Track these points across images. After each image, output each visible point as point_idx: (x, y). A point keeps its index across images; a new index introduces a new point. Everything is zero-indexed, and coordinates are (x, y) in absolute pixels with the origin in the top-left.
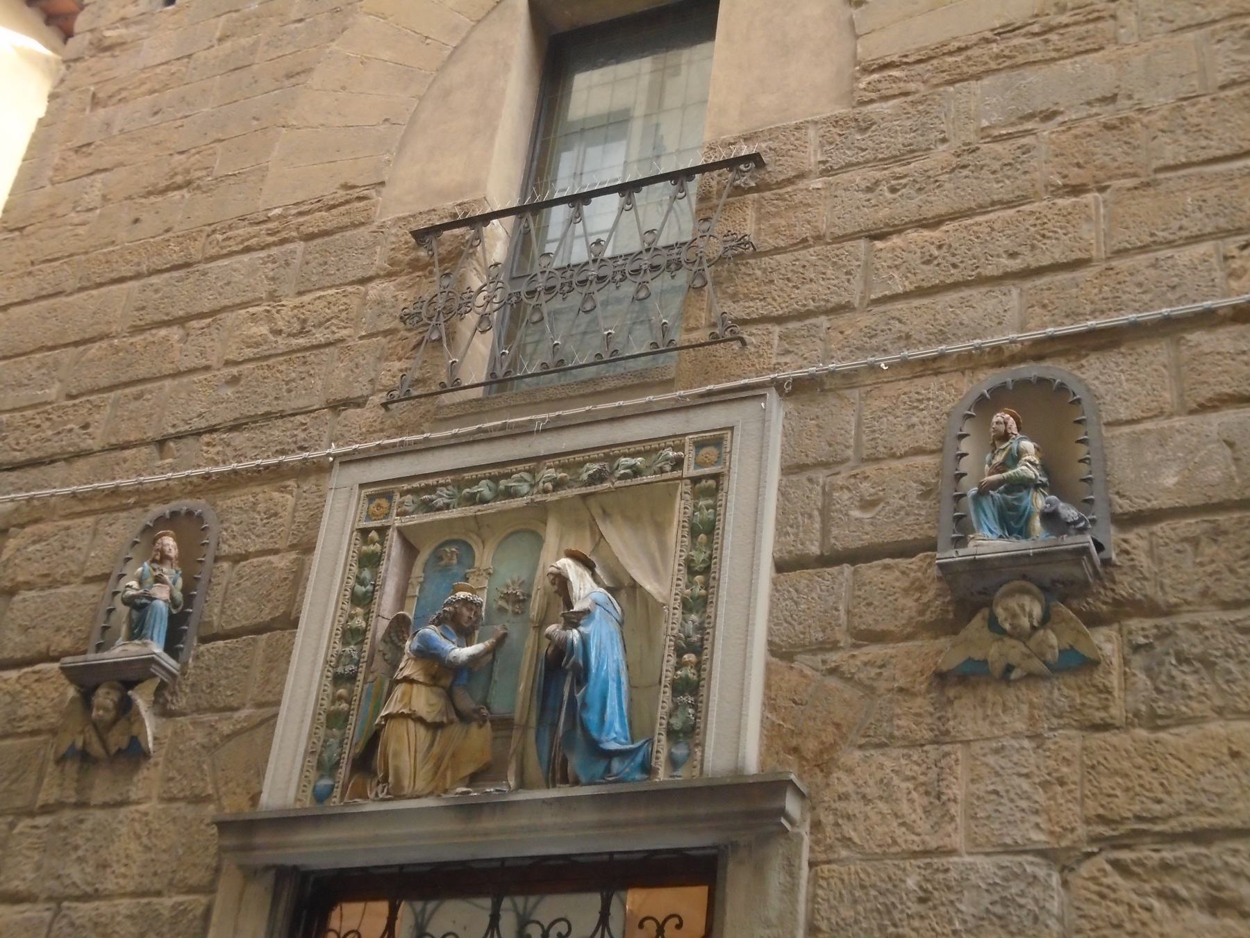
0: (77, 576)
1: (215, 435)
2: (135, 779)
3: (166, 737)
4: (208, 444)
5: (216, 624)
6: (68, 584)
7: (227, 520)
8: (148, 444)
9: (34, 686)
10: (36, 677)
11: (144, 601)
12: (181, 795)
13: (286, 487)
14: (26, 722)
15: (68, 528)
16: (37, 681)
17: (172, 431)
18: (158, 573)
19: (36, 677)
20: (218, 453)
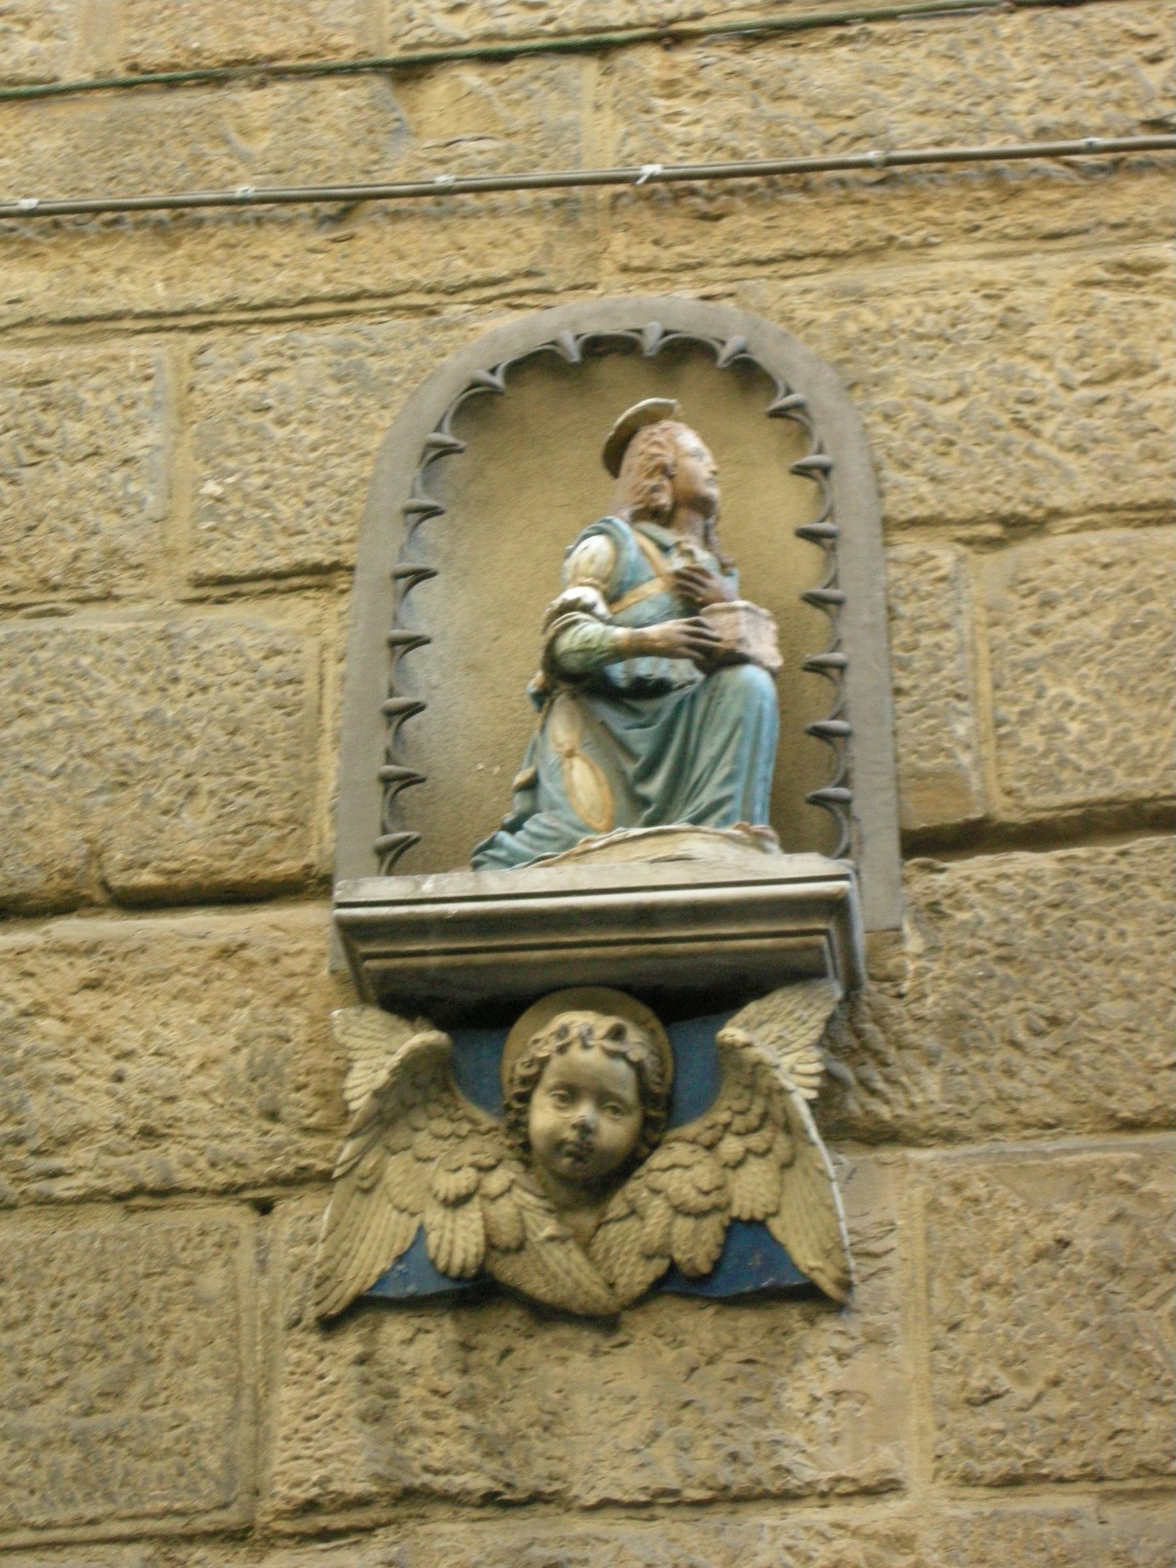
0: (139, 570)
1: (685, 57)
2: (795, 1400)
3: (891, 1228)
4: (670, 88)
5: (975, 785)
6: (108, 597)
7: (880, 381)
8: (353, 70)
9: (87, 1003)
10: (85, 969)
11: (682, 670)
12: (1067, 1462)
13: (1146, 269)
14: (80, 1155)
15: (36, 381)
16: (92, 985)
17: (456, 26)
18: (678, 563)
19: (85, 969)
20: (733, 123)
